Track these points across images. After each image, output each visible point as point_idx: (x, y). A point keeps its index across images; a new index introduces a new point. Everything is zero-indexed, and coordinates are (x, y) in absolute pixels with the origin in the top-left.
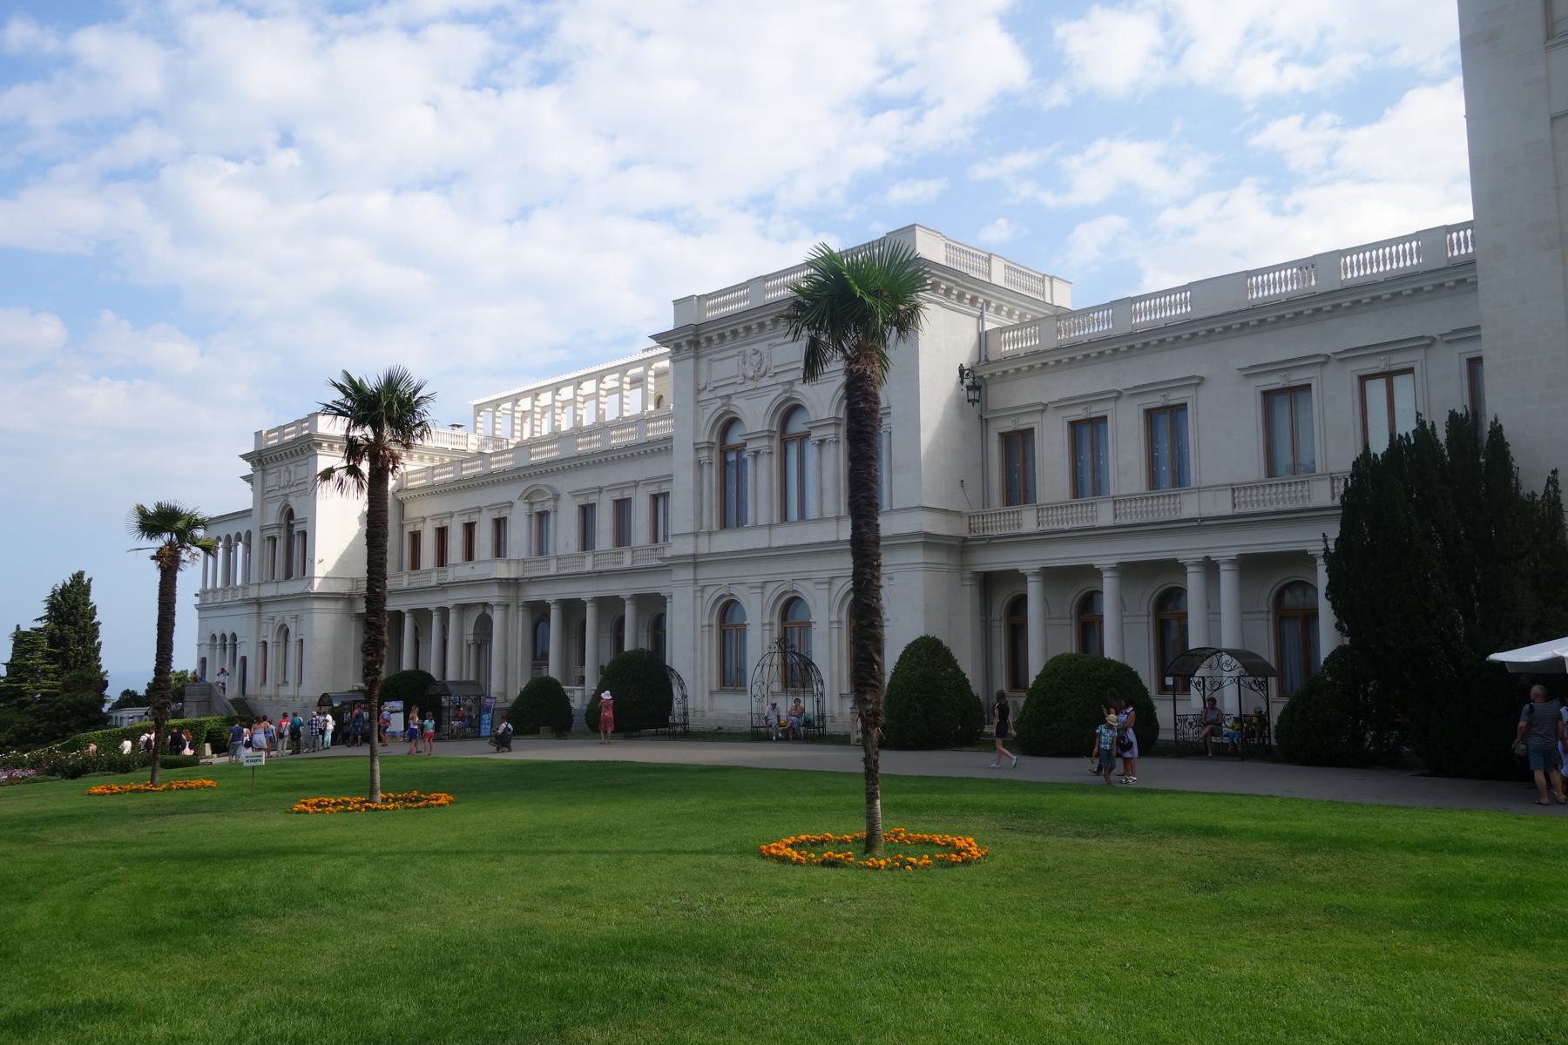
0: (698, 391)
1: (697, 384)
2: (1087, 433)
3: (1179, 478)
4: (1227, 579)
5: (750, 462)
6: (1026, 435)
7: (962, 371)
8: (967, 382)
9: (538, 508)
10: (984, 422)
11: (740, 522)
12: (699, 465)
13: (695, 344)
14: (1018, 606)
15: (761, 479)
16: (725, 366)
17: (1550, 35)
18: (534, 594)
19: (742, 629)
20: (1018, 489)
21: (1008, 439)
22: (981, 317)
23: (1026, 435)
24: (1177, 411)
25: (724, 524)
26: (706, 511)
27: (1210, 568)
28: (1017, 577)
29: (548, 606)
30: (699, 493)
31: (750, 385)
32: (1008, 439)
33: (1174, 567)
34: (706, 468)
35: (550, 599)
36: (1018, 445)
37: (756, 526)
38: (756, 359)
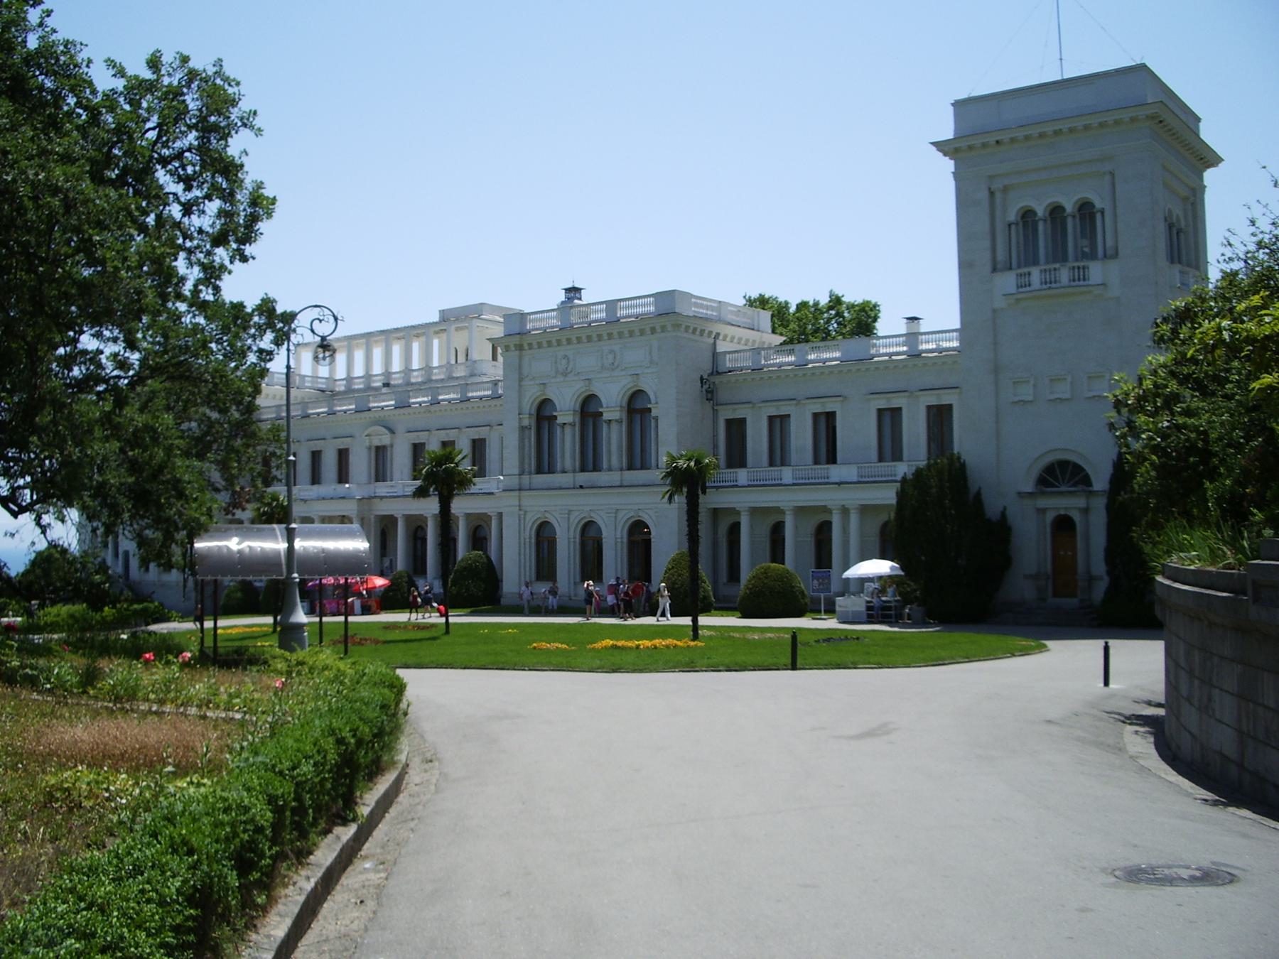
0: (521, 380)
1: (520, 373)
2: (778, 424)
3: (832, 459)
4: (854, 519)
5: (559, 430)
6: (742, 422)
7: (702, 379)
8: (705, 387)
9: (376, 442)
10: (715, 412)
11: (551, 471)
12: (522, 429)
13: (520, 348)
14: (735, 529)
15: (567, 445)
16: (540, 365)
17: (994, 270)
18: (385, 508)
19: (552, 542)
20: (737, 457)
21: (729, 423)
22: (715, 344)
23: (742, 422)
24: (831, 416)
25: (539, 471)
26: (527, 461)
27: (845, 511)
28: (734, 512)
29: (396, 519)
30: (521, 447)
31: (560, 378)
32: (729, 423)
33: (825, 510)
34: (527, 432)
35: (398, 514)
36: (736, 428)
37: (564, 472)
38: (564, 362)
